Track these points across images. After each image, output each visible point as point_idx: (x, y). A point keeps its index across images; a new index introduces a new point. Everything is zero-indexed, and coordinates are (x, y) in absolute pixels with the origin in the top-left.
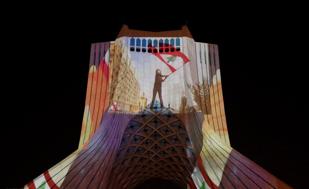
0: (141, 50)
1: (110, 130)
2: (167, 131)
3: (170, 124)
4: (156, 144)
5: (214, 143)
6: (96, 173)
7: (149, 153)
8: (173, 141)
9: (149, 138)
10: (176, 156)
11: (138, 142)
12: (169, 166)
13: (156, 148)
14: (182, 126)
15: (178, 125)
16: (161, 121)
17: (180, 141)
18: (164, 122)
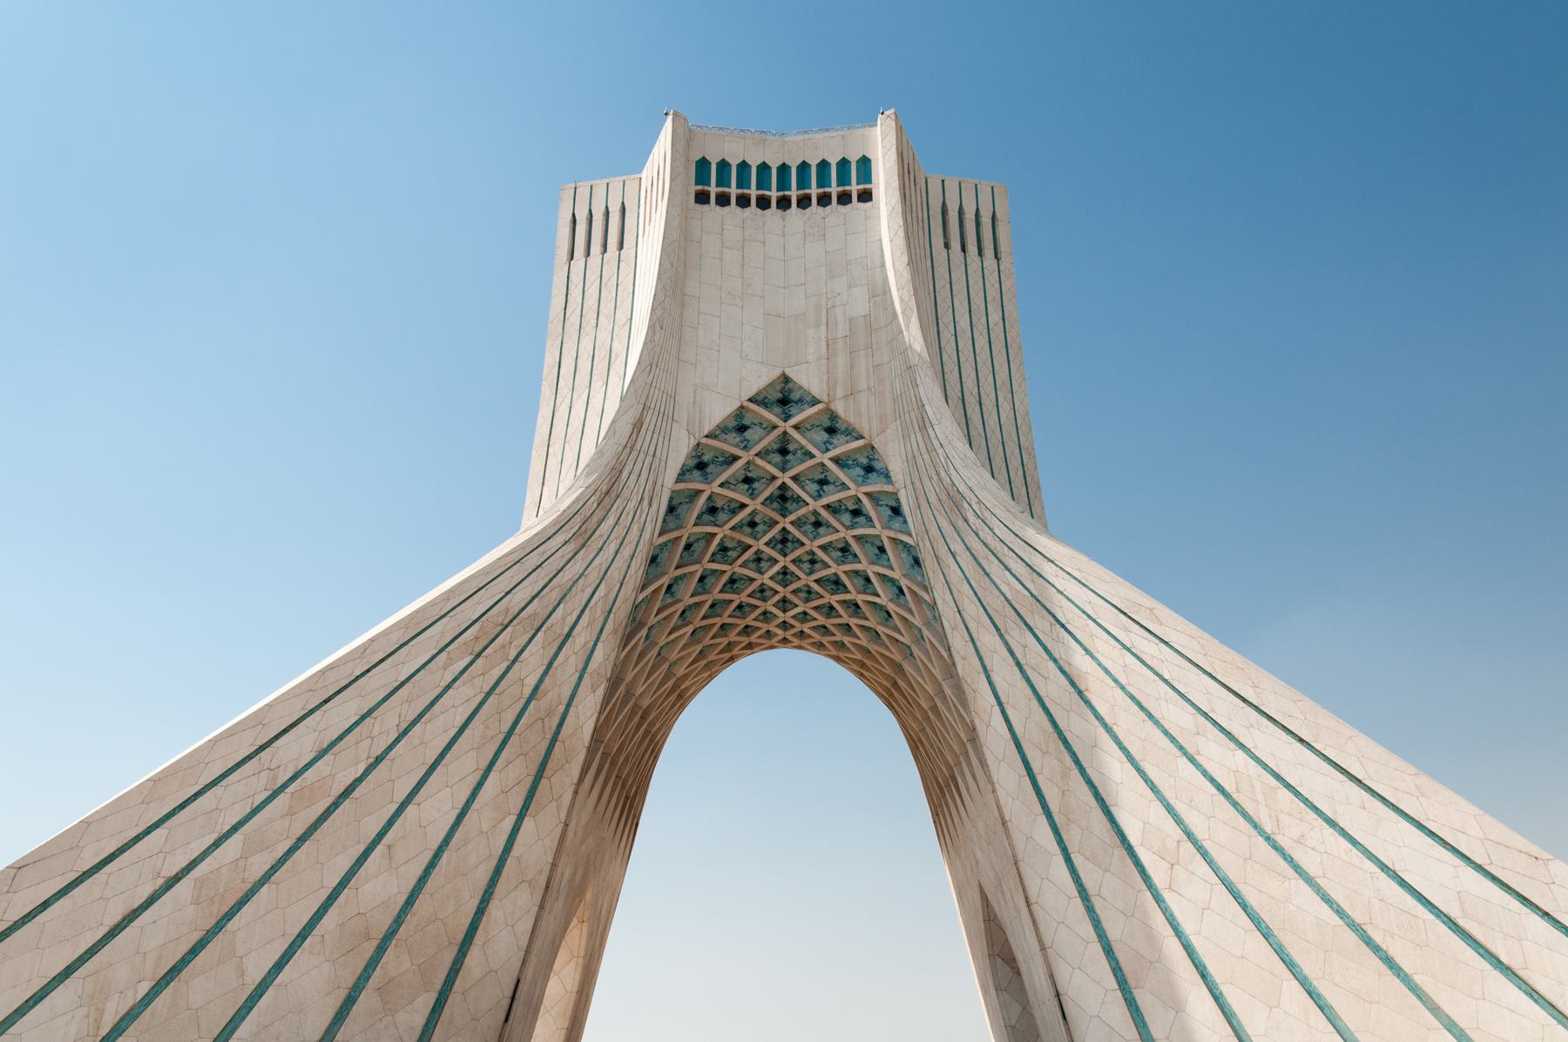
0: (733, 200)
1: (625, 474)
2: (823, 482)
3: (836, 460)
4: (784, 529)
5: (994, 523)
6: (579, 617)
7: (759, 560)
8: (846, 518)
9: (759, 507)
10: (857, 572)
11: (722, 516)
13: (784, 541)
14: (877, 465)
15: (864, 461)
16: (802, 448)
17: (870, 519)
18: (814, 451)
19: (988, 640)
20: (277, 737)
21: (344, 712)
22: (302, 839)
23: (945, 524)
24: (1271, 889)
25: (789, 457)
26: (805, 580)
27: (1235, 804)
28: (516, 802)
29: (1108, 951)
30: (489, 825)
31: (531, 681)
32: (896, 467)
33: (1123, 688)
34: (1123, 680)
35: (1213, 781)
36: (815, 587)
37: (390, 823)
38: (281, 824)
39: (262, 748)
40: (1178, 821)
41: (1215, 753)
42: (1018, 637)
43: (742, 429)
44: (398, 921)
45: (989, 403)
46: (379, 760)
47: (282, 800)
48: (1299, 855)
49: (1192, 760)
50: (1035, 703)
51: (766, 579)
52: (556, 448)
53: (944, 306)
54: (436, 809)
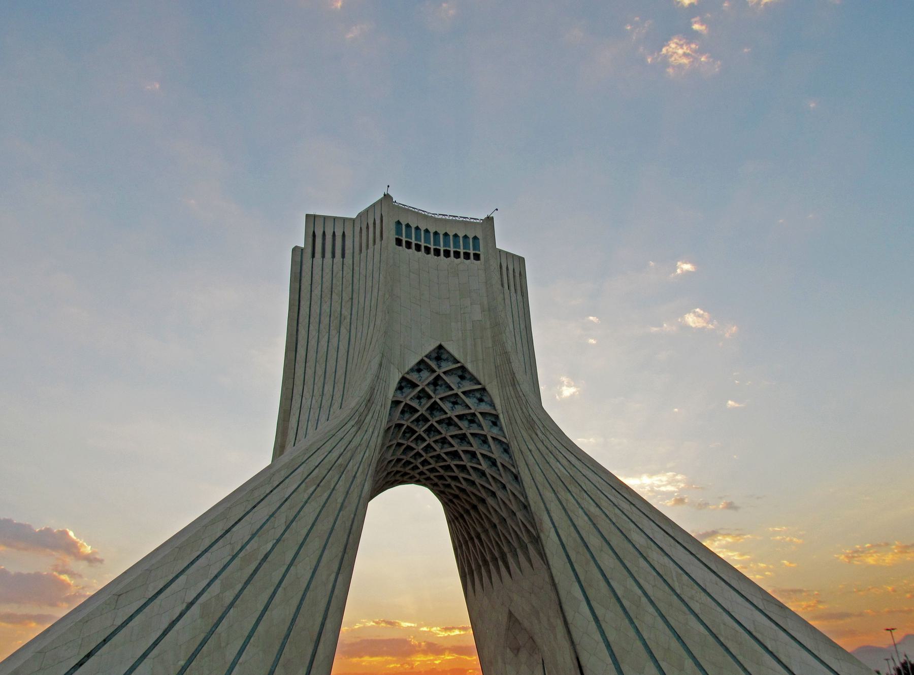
5: (551, 438)
14: (485, 399)
19: (548, 495)
20: (233, 526)
21: (262, 512)
23: (525, 435)
25: (438, 387)
27: (665, 581)
28: (335, 567)
29: (608, 646)
31: (340, 500)
32: (497, 402)
33: (614, 524)
34: (614, 520)
35: (654, 569)
36: (444, 456)
37: (284, 576)
39: (227, 531)
41: (655, 556)
42: (563, 494)
43: (419, 371)
44: (290, 630)
46: (278, 541)
47: (237, 561)
49: (645, 559)
50: (572, 529)
52: (311, 363)
54: (303, 569)
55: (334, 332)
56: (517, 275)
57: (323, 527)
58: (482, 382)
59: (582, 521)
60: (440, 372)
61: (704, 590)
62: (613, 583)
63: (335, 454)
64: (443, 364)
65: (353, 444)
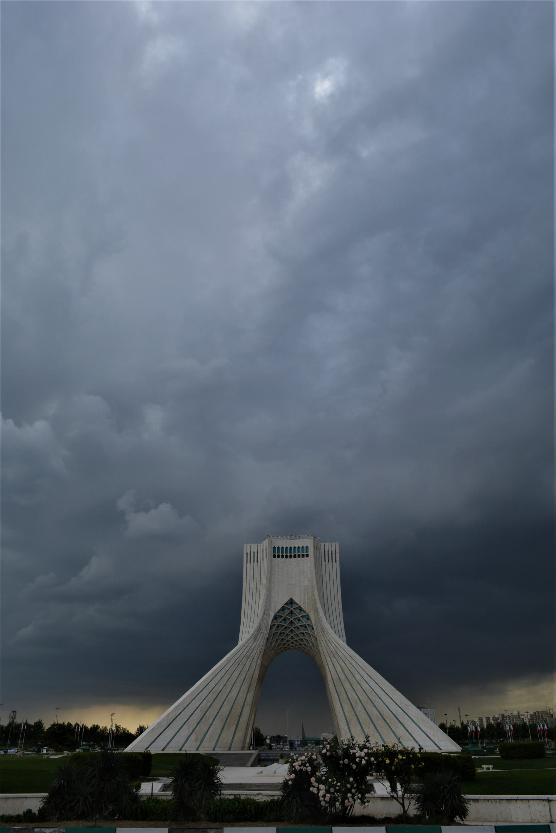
11: (280, 628)
12: (301, 644)
19: (328, 659)
21: (219, 677)
22: (215, 700)
24: (370, 708)
26: (296, 638)
28: (246, 691)
29: (346, 718)
30: (242, 694)
32: (313, 620)
38: (211, 697)
40: (357, 696)
42: (333, 659)
45: (333, 599)
48: (374, 703)
51: (288, 639)
53: (324, 577)
55: (254, 595)
56: (334, 553)
57: (242, 678)
58: (307, 611)
59: (339, 669)
60: (292, 609)
61: (380, 698)
62: (348, 694)
63: (246, 652)
64: (293, 605)
65: (252, 648)
